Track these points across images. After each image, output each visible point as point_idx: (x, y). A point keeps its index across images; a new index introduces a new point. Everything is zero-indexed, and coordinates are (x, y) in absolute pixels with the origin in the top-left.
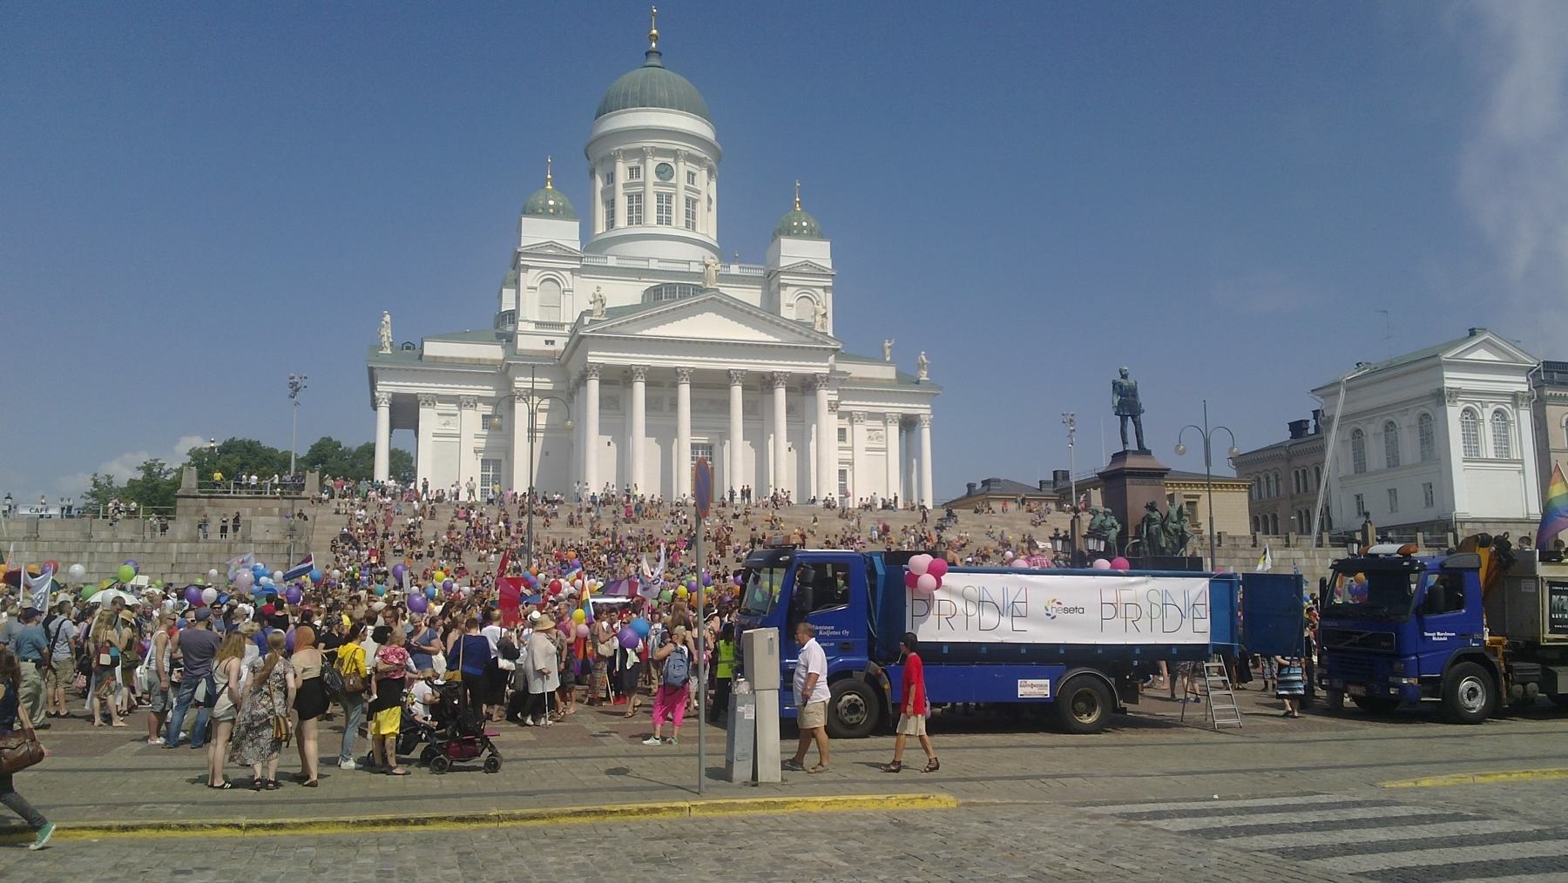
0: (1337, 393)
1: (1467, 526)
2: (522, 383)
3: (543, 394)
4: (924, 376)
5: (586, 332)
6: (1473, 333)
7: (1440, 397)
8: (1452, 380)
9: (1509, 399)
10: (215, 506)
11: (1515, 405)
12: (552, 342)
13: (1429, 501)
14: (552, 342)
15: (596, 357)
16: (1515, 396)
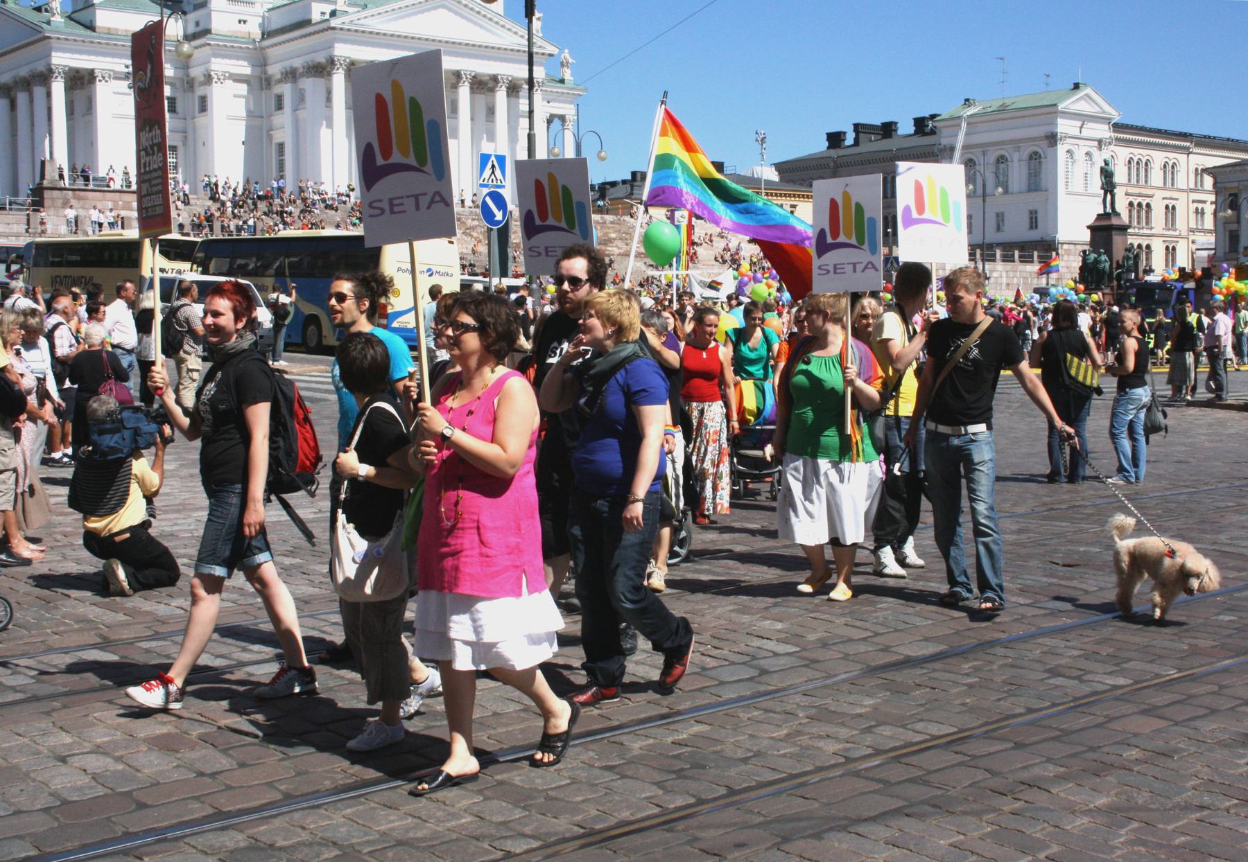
0: (959, 125)
1: (1065, 247)
2: (219, 65)
3: (238, 79)
4: (567, 74)
5: (335, 23)
6: (1076, 86)
7: (1052, 139)
8: (1064, 126)
9: (1096, 144)
10: (79, 199)
11: (1100, 148)
12: (245, 22)
13: (1033, 224)
14: (245, 22)
15: (343, 51)
16: (1100, 142)
